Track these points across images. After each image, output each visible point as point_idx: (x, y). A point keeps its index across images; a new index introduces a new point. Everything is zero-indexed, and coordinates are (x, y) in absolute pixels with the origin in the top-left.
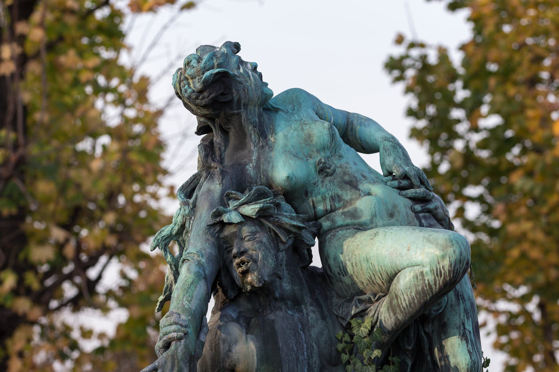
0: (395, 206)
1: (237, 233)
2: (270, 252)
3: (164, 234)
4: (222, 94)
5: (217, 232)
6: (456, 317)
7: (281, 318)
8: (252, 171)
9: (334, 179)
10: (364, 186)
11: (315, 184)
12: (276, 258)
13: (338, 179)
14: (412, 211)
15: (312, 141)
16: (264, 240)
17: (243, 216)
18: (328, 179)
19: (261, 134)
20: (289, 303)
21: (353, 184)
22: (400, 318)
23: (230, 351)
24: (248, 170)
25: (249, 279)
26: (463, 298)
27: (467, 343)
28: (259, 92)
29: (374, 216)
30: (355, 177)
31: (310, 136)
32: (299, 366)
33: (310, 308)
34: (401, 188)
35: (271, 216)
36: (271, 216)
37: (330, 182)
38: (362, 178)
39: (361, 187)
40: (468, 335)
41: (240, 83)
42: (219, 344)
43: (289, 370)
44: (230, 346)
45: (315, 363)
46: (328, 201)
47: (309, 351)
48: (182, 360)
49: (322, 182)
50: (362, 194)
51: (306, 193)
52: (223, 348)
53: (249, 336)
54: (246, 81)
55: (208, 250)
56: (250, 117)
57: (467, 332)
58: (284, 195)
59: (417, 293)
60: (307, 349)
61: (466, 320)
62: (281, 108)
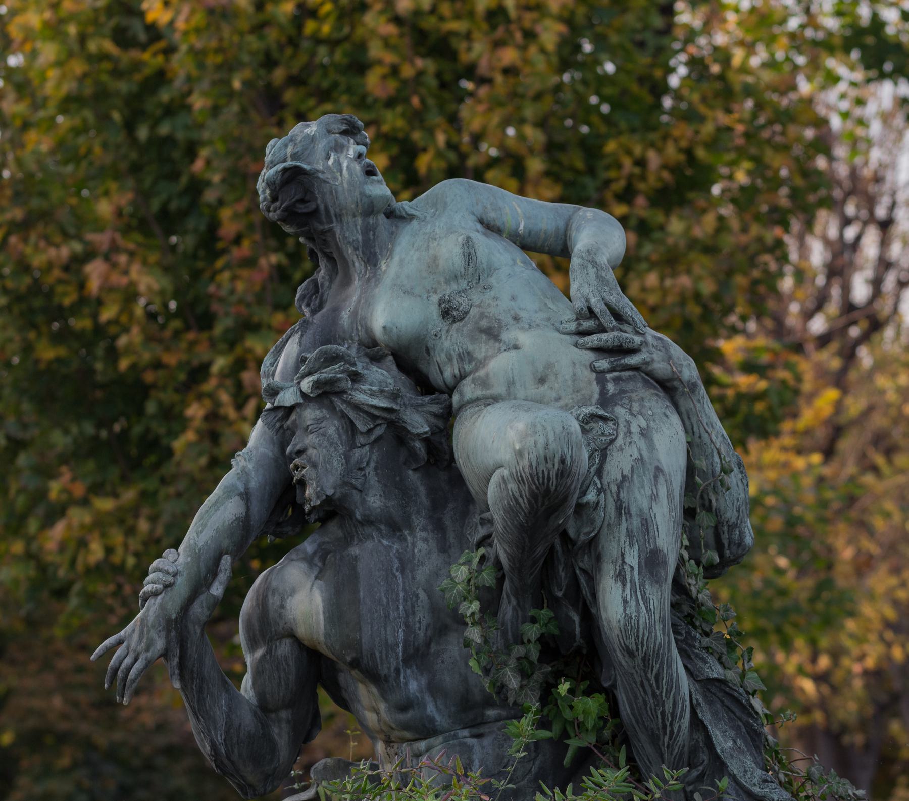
0: (549, 366)
1: (298, 422)
2: (336, 450)
4: (302, 201)
5: (278, 420)
6: (613, 544)
7: (370, 553)
8: (346, 320)
9: (463, 326)
10: (511, 335)
11: (436, 335)
12: (345, 458)
13: (470, 326)
14: (592, 370)
15: (437, 266)
16: (331, 431)
18: (455, 326)
19: (368, 260)
20: (382, 527)
21: (492, 333)
23: (282, 606)
24: (342, 318)
26: (628, 513)
27: (624, 585)
28: (357, 194)
29: (511, 384)
30: (499, 321)
31: (435, 258)
32: (388, 629)
33: (420, 534)
35: (344, 392)
36: (344, 392)
37: (457, 330)
38: (512, 322)
39: (505, 336)
41: (325, 182)
42: (267, 596)
43: (371, 635)
44: (283, 599)
45: (420, 622)
46: (455, 362)
47: (409, 603)
48: (153, 627)
49: (448, 331)
50: (503, 349)
52: (274, 601)
53: (319, 582)
54: (335, 178)
55: (261, 450)
56: (347, 234)
57: (627, 568)
58: (393, 354)
60: (405, 600)
61: (628, 547)
62: (417, 213)
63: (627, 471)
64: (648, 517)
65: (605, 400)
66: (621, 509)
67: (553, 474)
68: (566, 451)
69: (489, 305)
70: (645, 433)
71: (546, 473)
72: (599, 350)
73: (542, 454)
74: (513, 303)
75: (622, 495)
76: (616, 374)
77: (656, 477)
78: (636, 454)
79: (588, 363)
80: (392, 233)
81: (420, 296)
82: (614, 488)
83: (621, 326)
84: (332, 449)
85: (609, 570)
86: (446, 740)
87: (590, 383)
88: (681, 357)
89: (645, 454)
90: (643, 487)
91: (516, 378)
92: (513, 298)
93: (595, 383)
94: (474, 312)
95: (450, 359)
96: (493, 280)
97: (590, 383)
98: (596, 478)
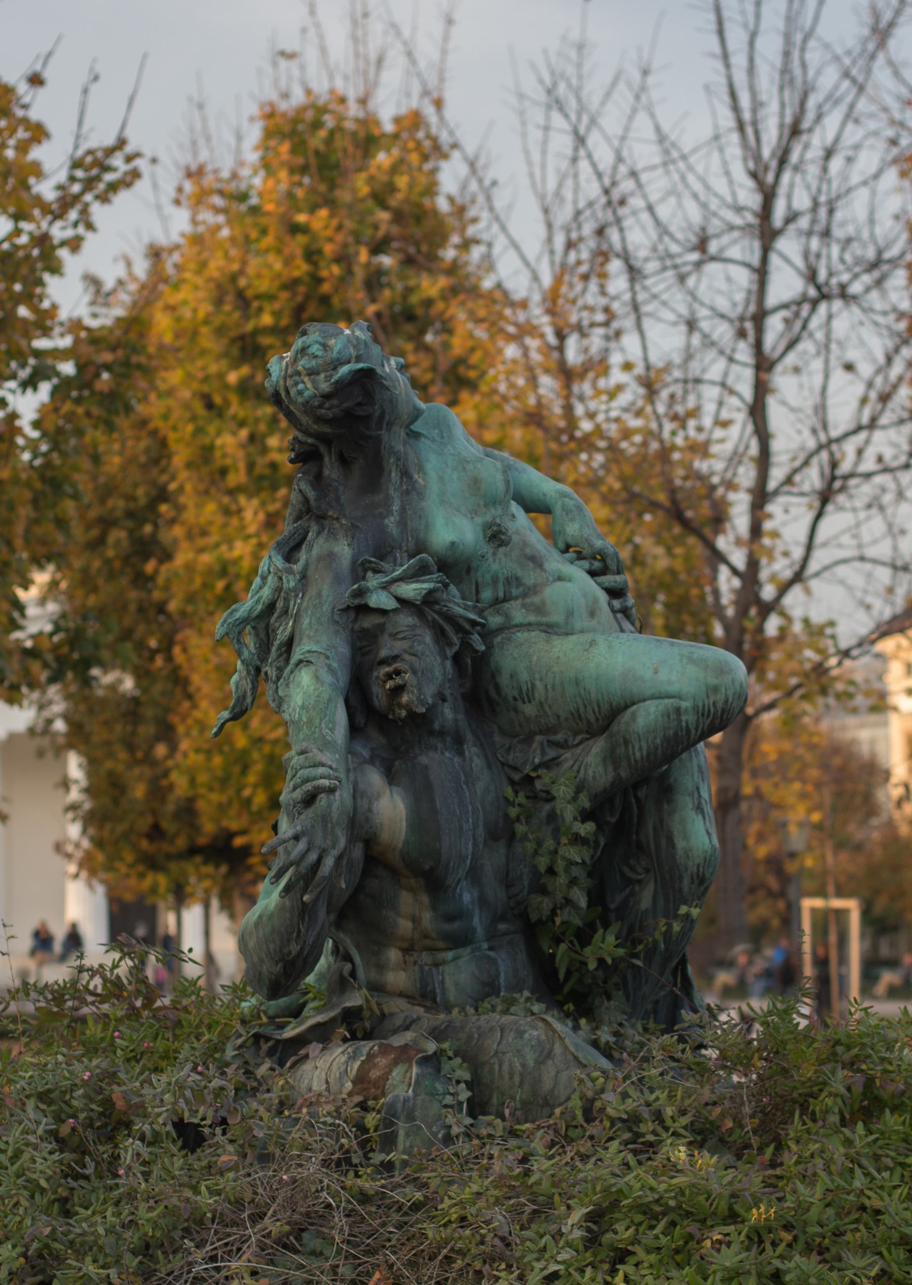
0: (596, 601)
3: (237, 615)
4: (359, 404)
17: (399, 600)
18: (502, 550)
20: (449, 739)
22: (624, 774)
23: (370, 810)
25: (405, 698)
29: (570, 614)
33: (474, 750)
34: (593, 574)
35: (437, 602)
36: (437, 602)
37: (505, 555)
39: (547, 566)
41: (387, 389)
44: (370, 803)
49: (494, 554)
51: (469, 570)
59: (666, 739)
85: (686, 802)
86: (473, 951)
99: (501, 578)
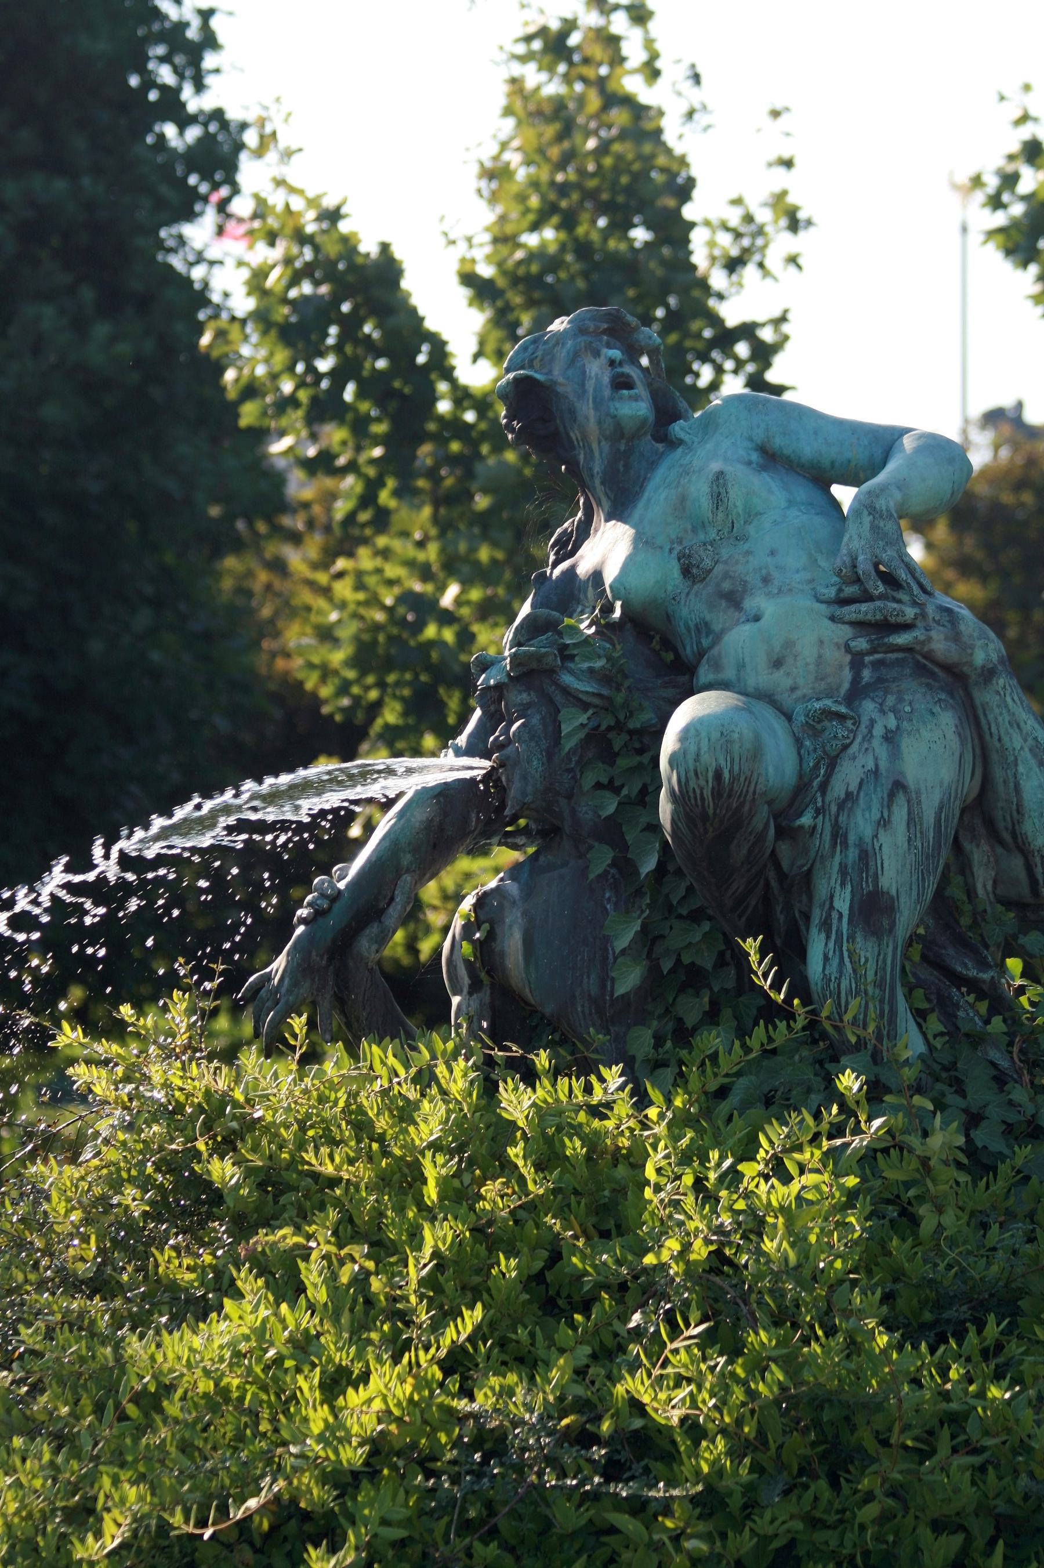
0: (789, 644)
10: (755, 602)
15: (684, 509)
26: (845, 844)
27: (828, 937)
31: (683, 499)
32: (592, 976)
38: (760, 584)
39: (750, 604)
40: (835, 922)
49: (688, 594)
57: (835, 915)
61: (838, 888)
63: (853, 787)
64: (870, 848)
65: (856, 693)
66: (839, 836)
67: (708, 793)
68: (722, 763)
69: (737, 562)
70: (891, 738)
71: (698, 792)
72: (860, 625)
73: (692, 768)
74: (769, 559)
75: (840, 819)
76: (878, 656)
77: (892, 795)
78: (870, 765)
79: (842, 641)
80: (653, 463)
81: (661, 548)
82: (834, 809)
83: (895, 594)
84: (533, 744)
87: (841, 667)
88: (975, 635)
89: (883, 765)
90: (869, 809)
91: (747, 660)
92: (772, 553)
93: (847, 669)
94: (719, 569)
95: (689, 630)
96: (751, 529)
97: (841, 667)
98: (819, 794)
99: (692, 625)
